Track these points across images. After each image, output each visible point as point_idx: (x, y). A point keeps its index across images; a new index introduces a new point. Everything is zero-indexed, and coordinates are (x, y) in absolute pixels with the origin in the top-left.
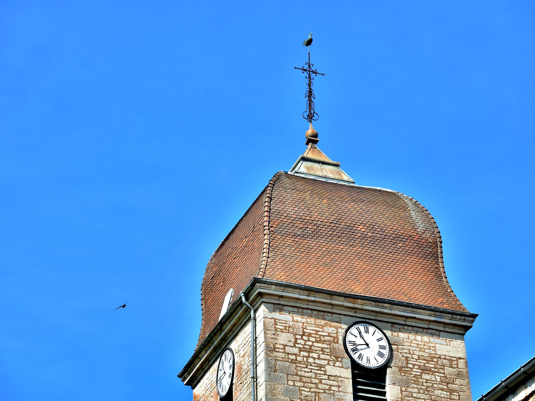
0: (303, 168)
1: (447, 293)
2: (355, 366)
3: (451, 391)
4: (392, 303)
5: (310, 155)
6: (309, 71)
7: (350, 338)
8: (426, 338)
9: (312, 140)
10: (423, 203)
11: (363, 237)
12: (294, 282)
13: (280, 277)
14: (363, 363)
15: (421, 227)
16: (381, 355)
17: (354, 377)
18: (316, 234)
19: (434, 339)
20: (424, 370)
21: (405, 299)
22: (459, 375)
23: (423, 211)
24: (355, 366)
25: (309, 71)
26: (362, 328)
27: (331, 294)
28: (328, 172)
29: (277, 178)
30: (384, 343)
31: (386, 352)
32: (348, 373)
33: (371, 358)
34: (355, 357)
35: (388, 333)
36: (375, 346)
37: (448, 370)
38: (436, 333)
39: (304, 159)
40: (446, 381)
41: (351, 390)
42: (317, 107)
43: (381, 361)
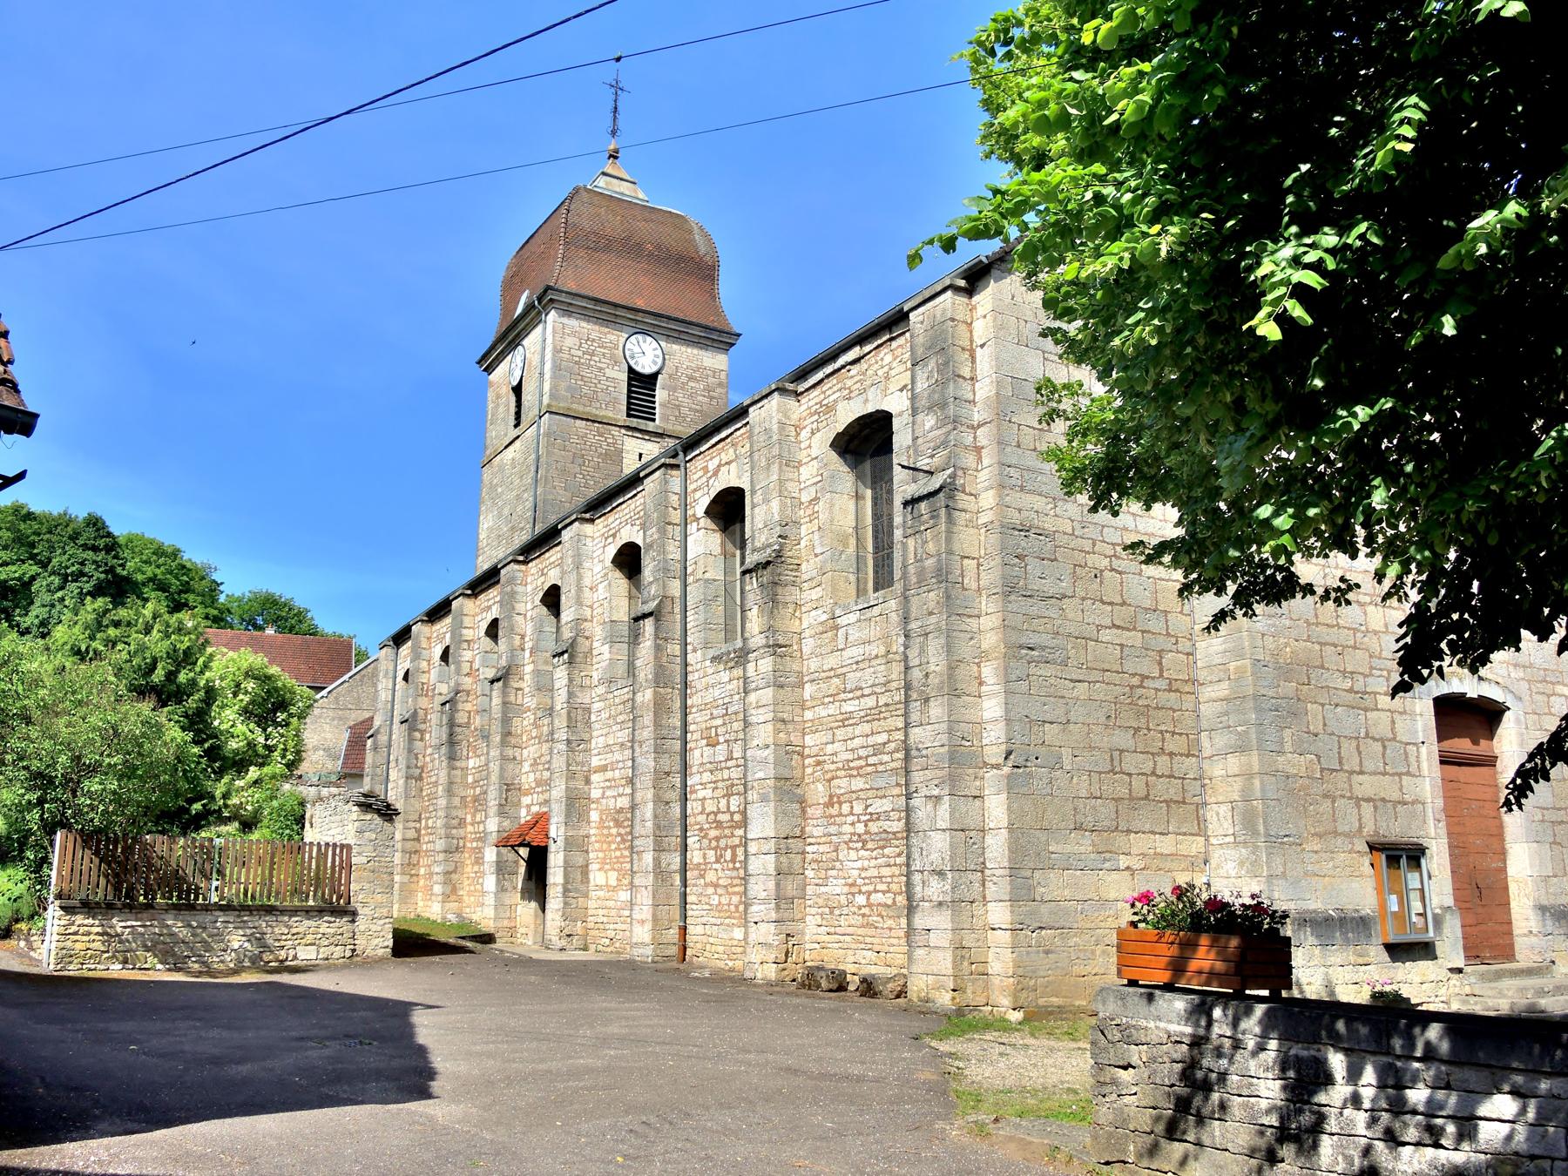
0: (602, 182)
1: (717, 311)
2: (631, 370)
3: (712, 398)
4: (669, 318)
5: (610, 171)
6: (617, 87)
7: (628, 345)
8: (695, 351)
9: (614, 156)
10: (707, 228)
11: (651, 254)
12: (583, 292)
13: (571, 286)
14: (638, 369)
15: (702, 250)
16: (655, 363)
17: (629, 379)
18: (607, 248)
19: (702, 352)
20: (691, 378)
21: (681, 316)
22: (720, 385)
23: (706, 236)
24: (631, 370)
25: (617, 87)
26: (640, 337)
27: (616, 305)
28: (624, 189)
29: (577, 191)
30: (659, 352)
31: (660, 361)
32: (625, 376)
33: (646, 366)
34: (632, 363)
35: (663, 344)
36: (650, 354)
37: (711, 380)
38: (705, 347)
39: (604, 174)
40: (708, 389)
41: (625, 391)
42: (621, 123)
43: (654, 369)
